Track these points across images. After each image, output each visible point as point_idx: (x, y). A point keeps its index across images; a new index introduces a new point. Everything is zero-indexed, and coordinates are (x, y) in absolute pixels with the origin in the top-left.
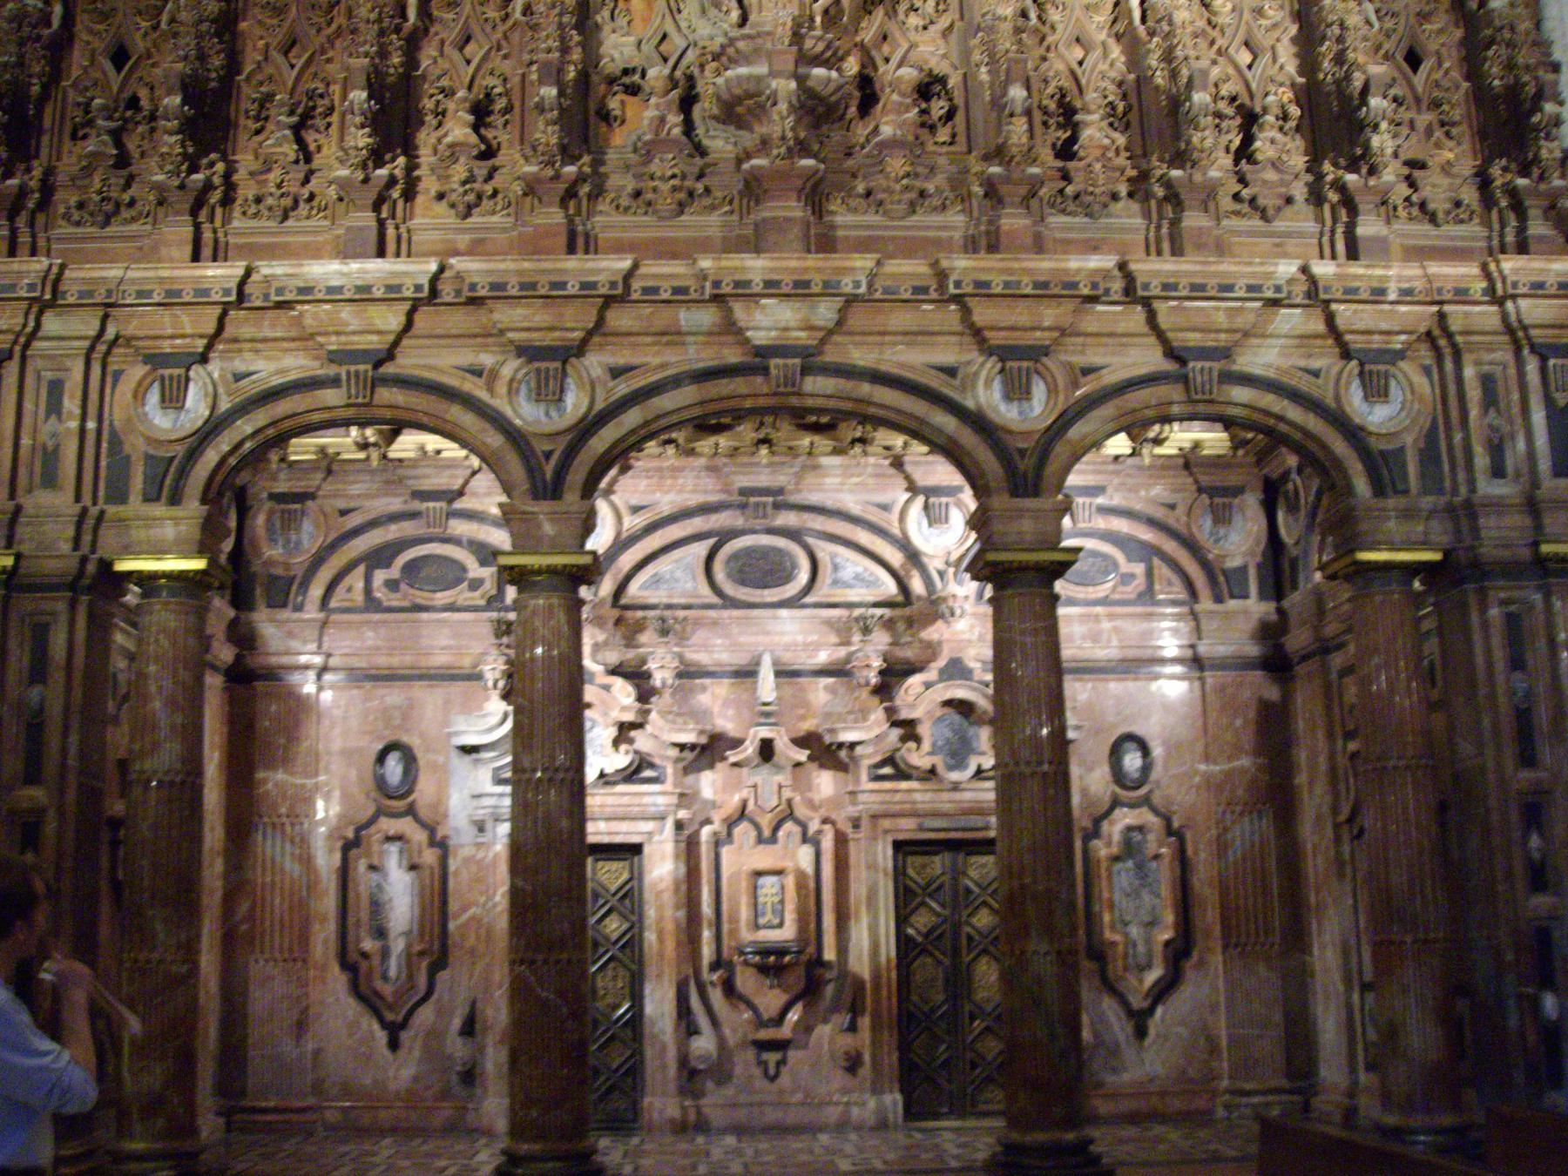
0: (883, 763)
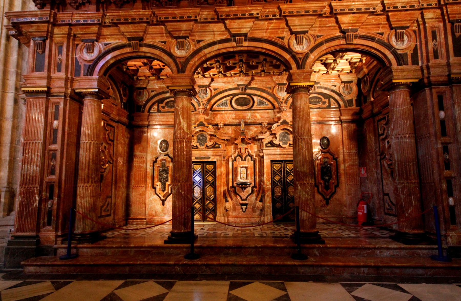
0: (268, 143)
